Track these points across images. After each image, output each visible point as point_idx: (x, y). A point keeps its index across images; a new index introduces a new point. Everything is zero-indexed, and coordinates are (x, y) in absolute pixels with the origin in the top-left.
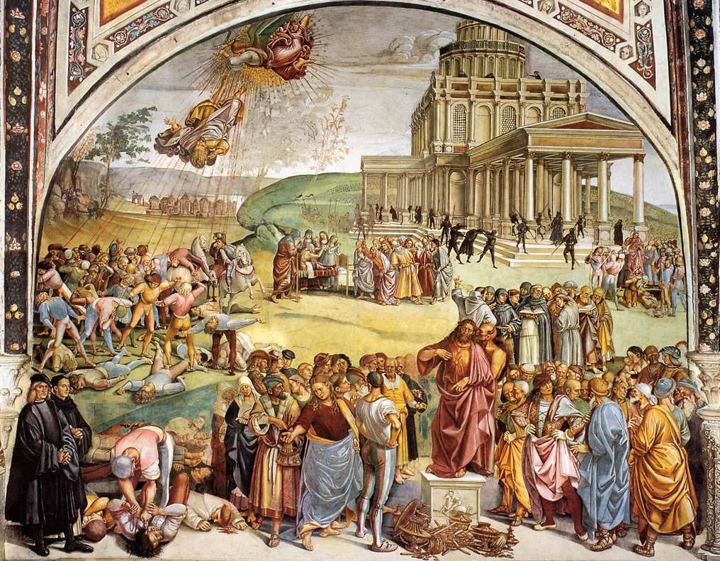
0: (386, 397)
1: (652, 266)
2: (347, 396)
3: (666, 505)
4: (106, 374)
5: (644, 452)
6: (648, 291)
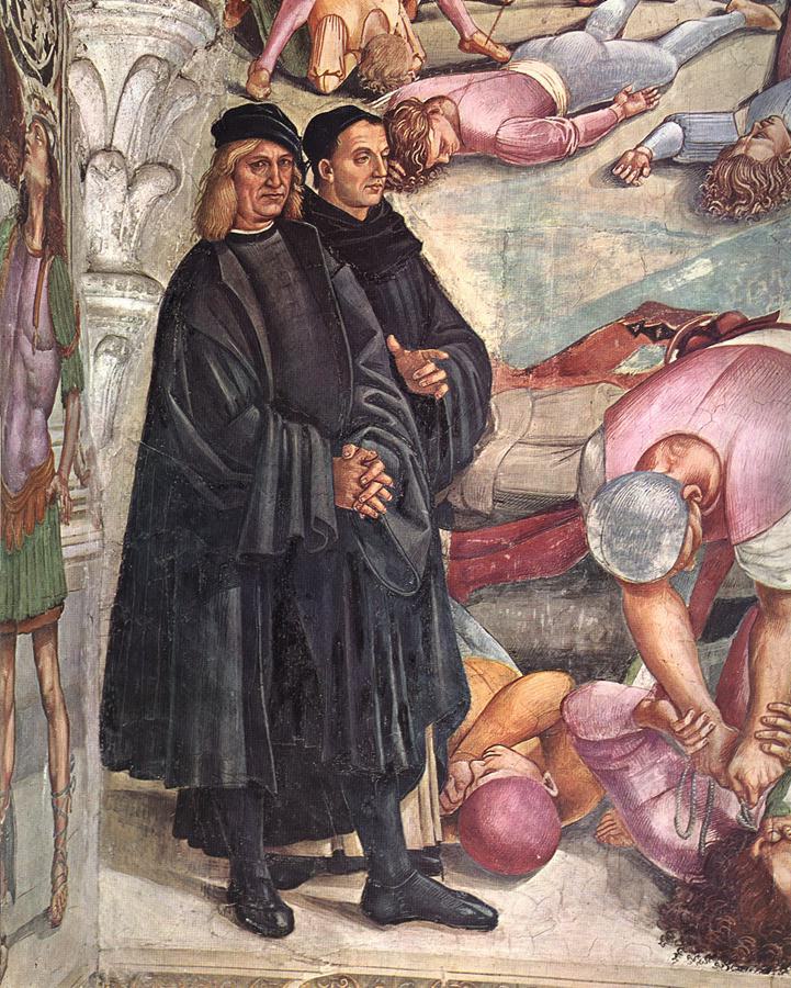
4: (557, 89)
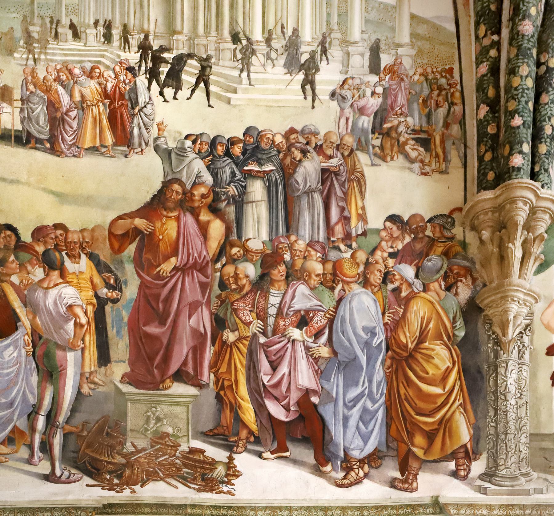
0: (67, 282)
1: (419, 104)
2: (15, 279)
3: (433, 423)
5: (405, 354)
6: (413, 139)
